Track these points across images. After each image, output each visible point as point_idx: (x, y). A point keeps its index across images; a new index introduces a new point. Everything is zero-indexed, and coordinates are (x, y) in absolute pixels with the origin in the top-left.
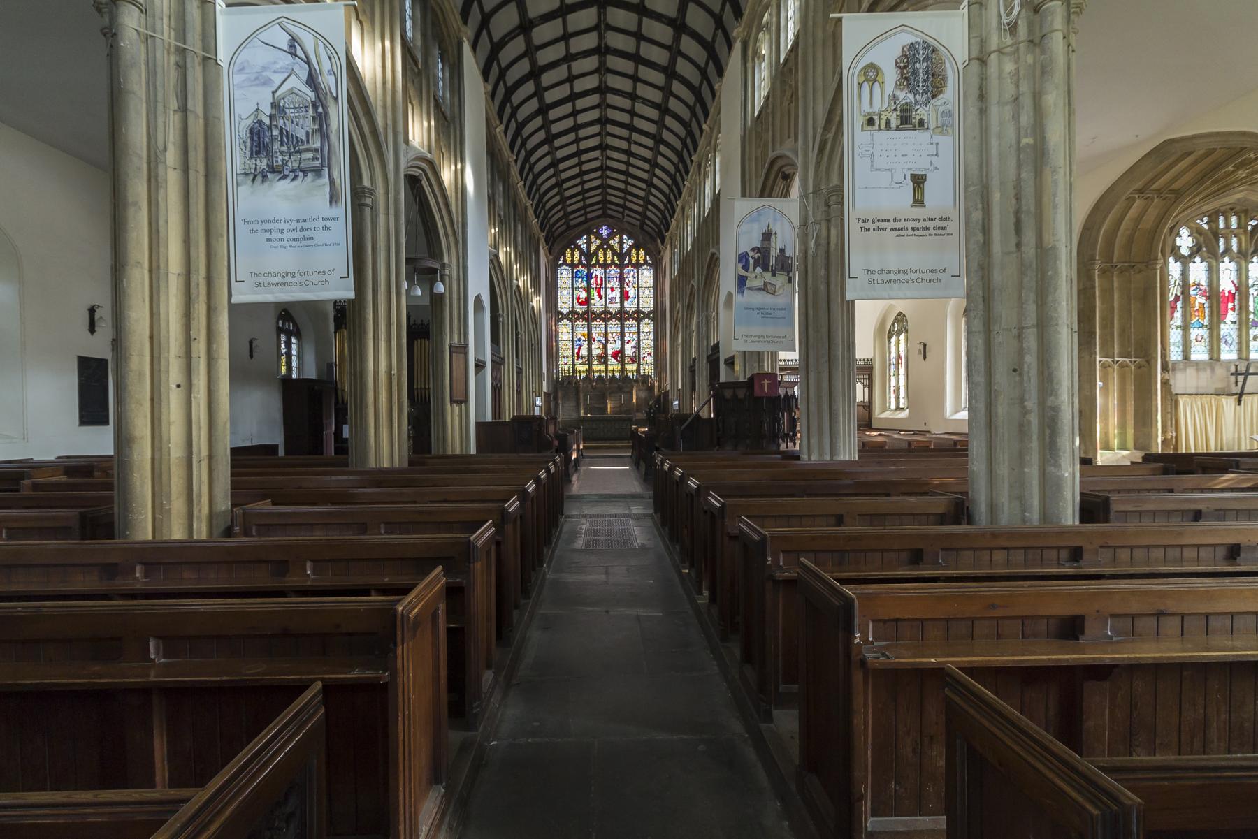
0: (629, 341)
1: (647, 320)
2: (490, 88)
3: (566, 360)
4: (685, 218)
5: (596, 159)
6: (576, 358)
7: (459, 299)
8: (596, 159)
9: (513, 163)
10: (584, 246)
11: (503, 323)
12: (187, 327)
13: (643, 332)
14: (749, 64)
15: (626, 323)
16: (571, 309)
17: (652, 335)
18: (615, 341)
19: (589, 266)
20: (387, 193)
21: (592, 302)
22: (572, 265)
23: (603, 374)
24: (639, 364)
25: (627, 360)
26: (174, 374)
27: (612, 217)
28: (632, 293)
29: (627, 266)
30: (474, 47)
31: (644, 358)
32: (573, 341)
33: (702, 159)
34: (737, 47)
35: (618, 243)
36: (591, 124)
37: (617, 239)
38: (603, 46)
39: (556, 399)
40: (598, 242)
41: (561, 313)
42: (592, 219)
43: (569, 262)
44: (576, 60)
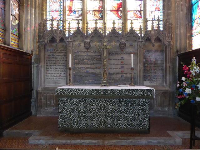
6: (67, 12)
25: (130, 16)
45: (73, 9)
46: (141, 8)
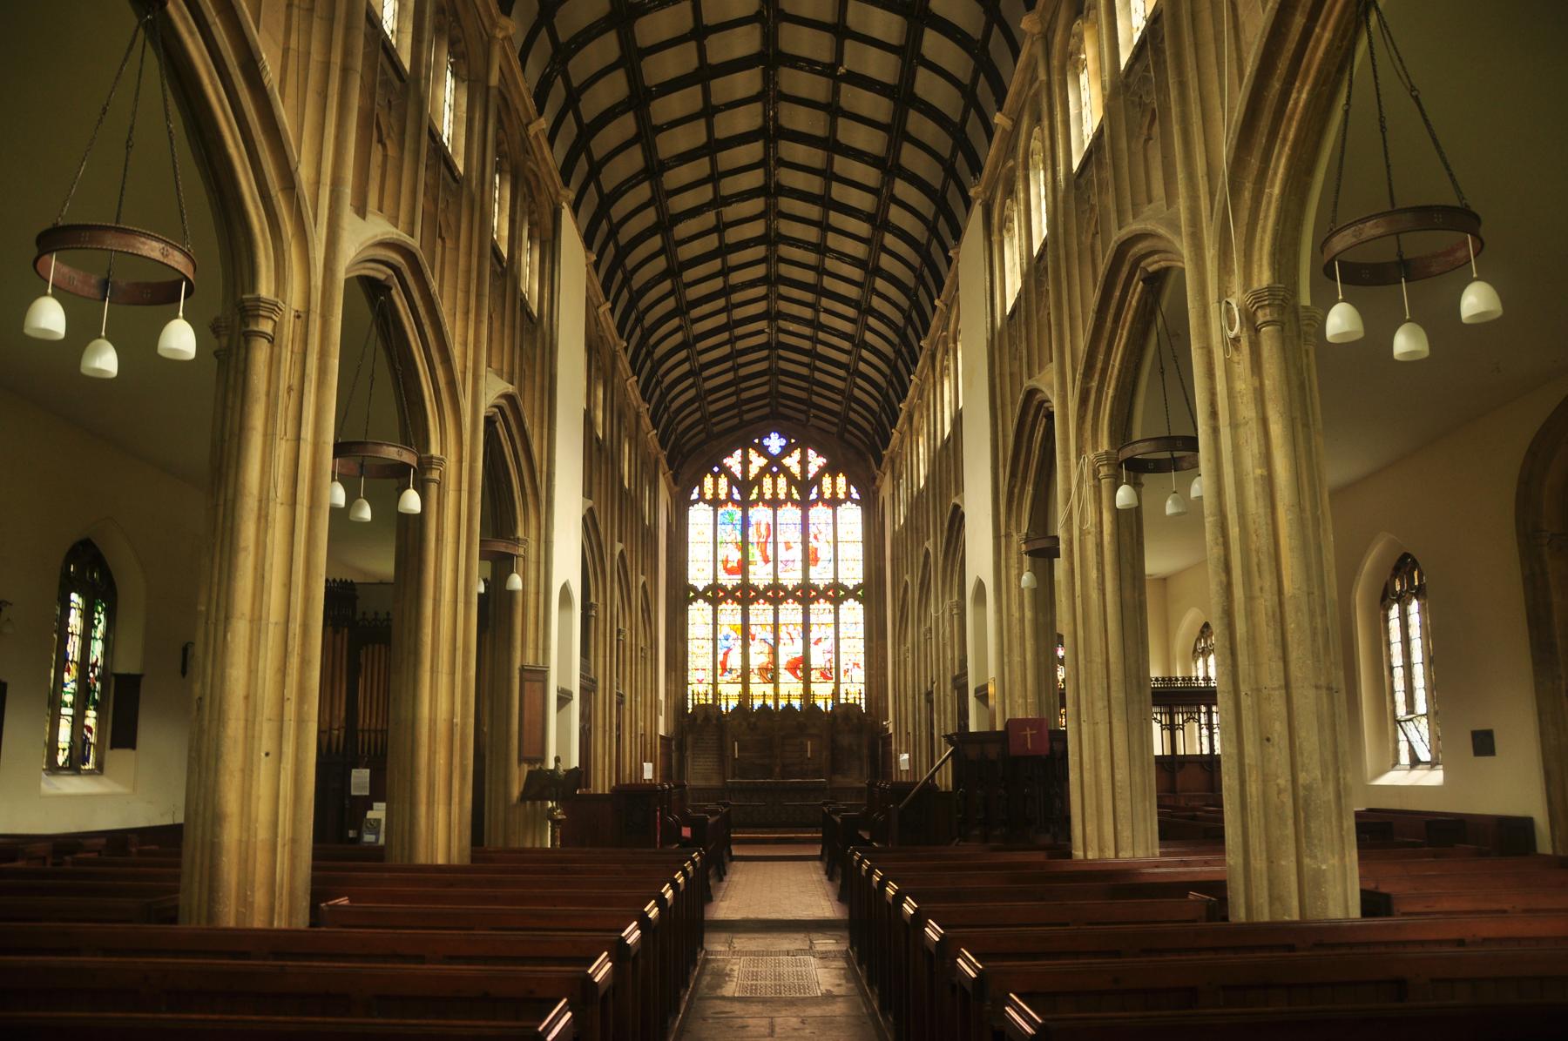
0: (819, 640)
2: (594, 258)
3: (700, 675)
4: (915, 433)
5: (761, 332)
6: (719, 671)
7: (538, 593)
8: (761, 332)
9: (622, 352)
10: (737, 470)
11: (596, 618)
12: (282, 684)
14: (995, 238)
19: (745, 504)
20: (460, 461)
22: (715, 503)
23: (770, 702)
24: (837, 683)
25: (815, 675)
26: (266, 742)
27: (788, 418)
28: (825, 552)
29: (814, 503)
30: (575, 209)
31: (846, 671)
32: (715, 639)
33: (936, 348)
34: (977, 211)
36: (752, 284)
37: (797, 454)
38: (773, 185)
39: (681, 747)
40: (763, 461)
41: (694, 589)
42: (751, 422)
43: (709, 496)
44: (730, 204)
45: (728, 667)
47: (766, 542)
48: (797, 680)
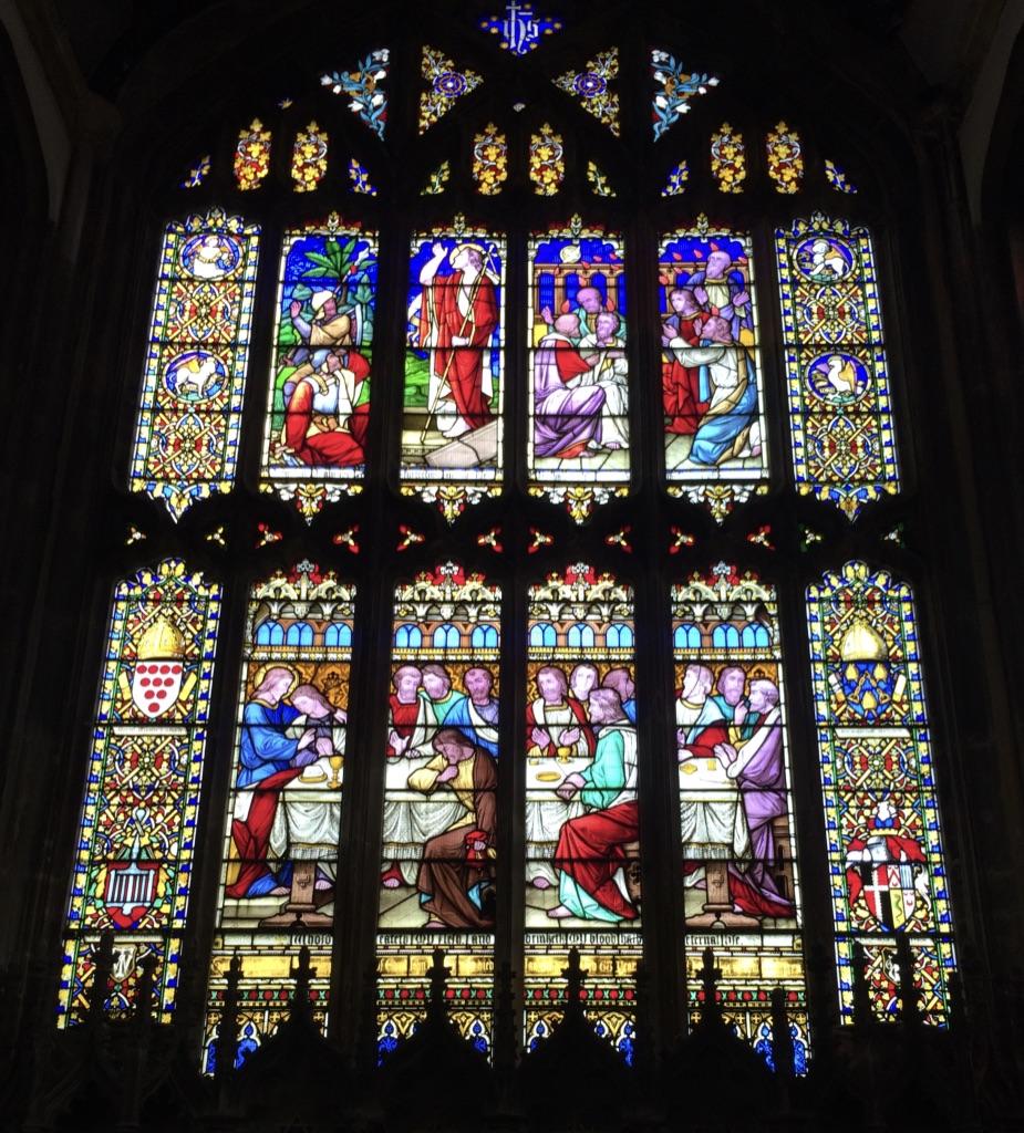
0: (722, 726)
1: (855, 572)
6: (229, 874)
10: (368, 101)
13: (836, 663)
15: (682, 594)
16: (225, 488)
17: (908, 685)
18: (590, 730)
21: (410, 439)
23: (473, 1026)
28: (725, 379)
35: (612, 86)
41: (152, 511)
46: (783, 843)
47: (477, 349)
48: (607, 918)
